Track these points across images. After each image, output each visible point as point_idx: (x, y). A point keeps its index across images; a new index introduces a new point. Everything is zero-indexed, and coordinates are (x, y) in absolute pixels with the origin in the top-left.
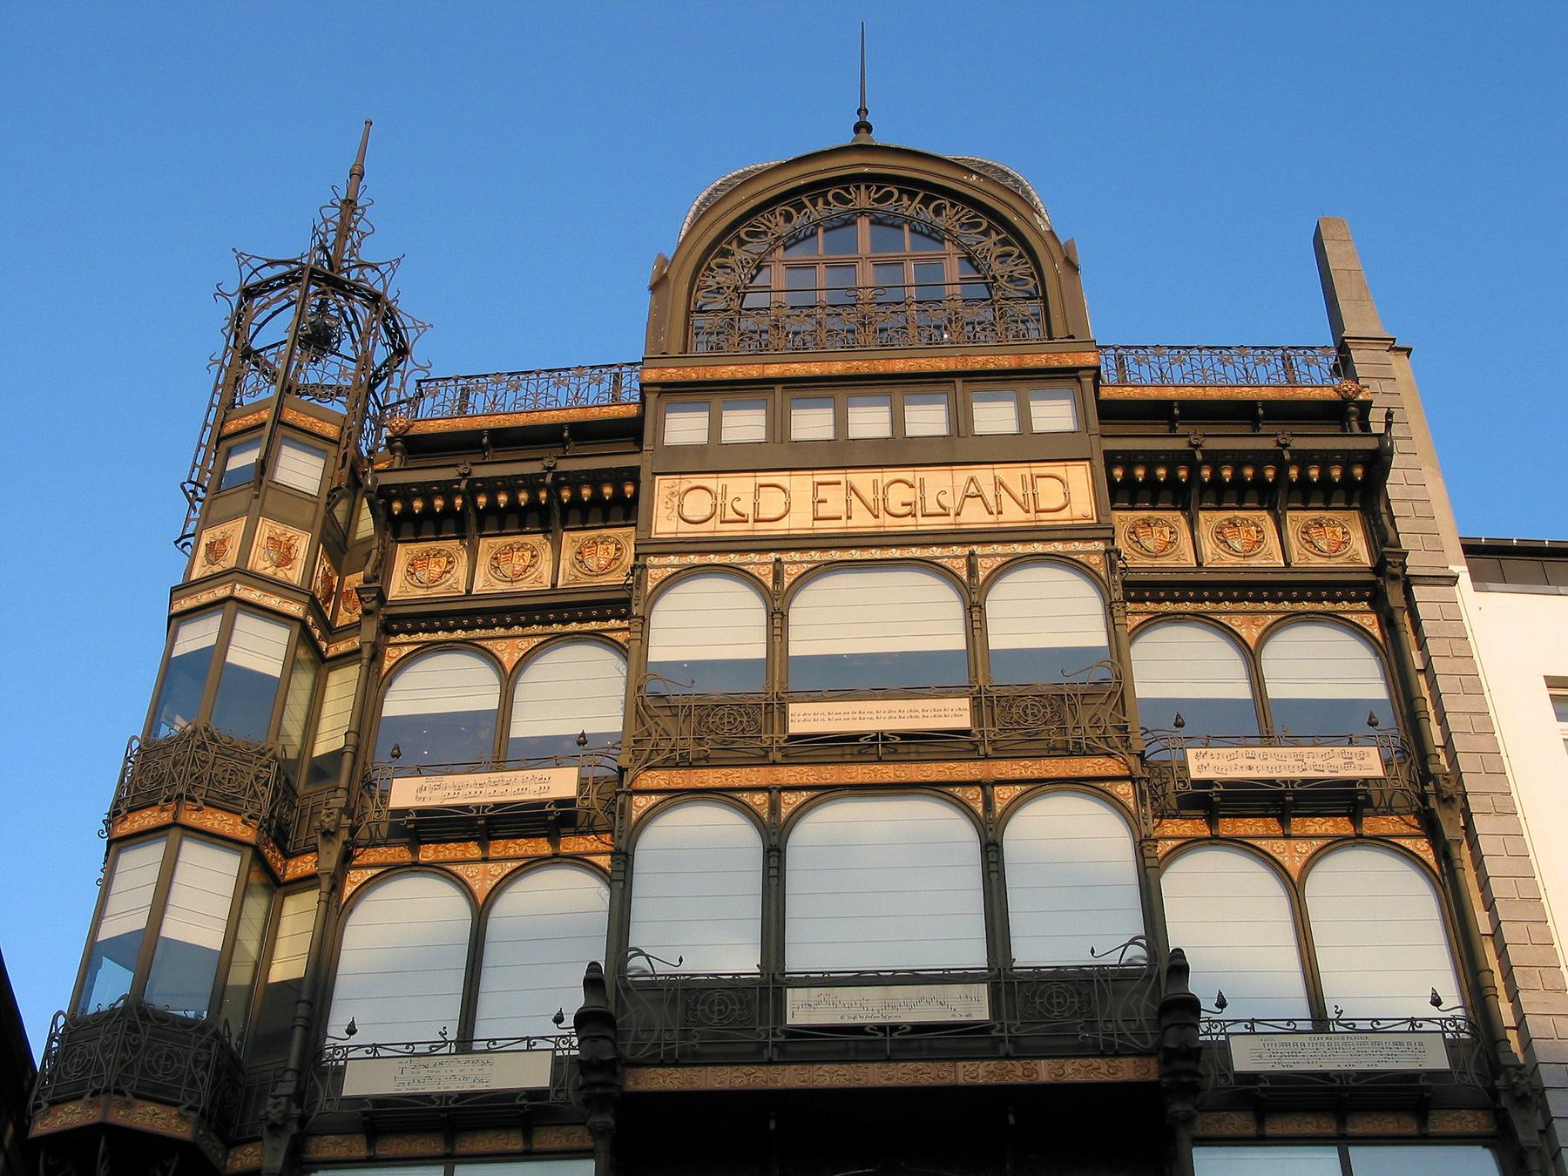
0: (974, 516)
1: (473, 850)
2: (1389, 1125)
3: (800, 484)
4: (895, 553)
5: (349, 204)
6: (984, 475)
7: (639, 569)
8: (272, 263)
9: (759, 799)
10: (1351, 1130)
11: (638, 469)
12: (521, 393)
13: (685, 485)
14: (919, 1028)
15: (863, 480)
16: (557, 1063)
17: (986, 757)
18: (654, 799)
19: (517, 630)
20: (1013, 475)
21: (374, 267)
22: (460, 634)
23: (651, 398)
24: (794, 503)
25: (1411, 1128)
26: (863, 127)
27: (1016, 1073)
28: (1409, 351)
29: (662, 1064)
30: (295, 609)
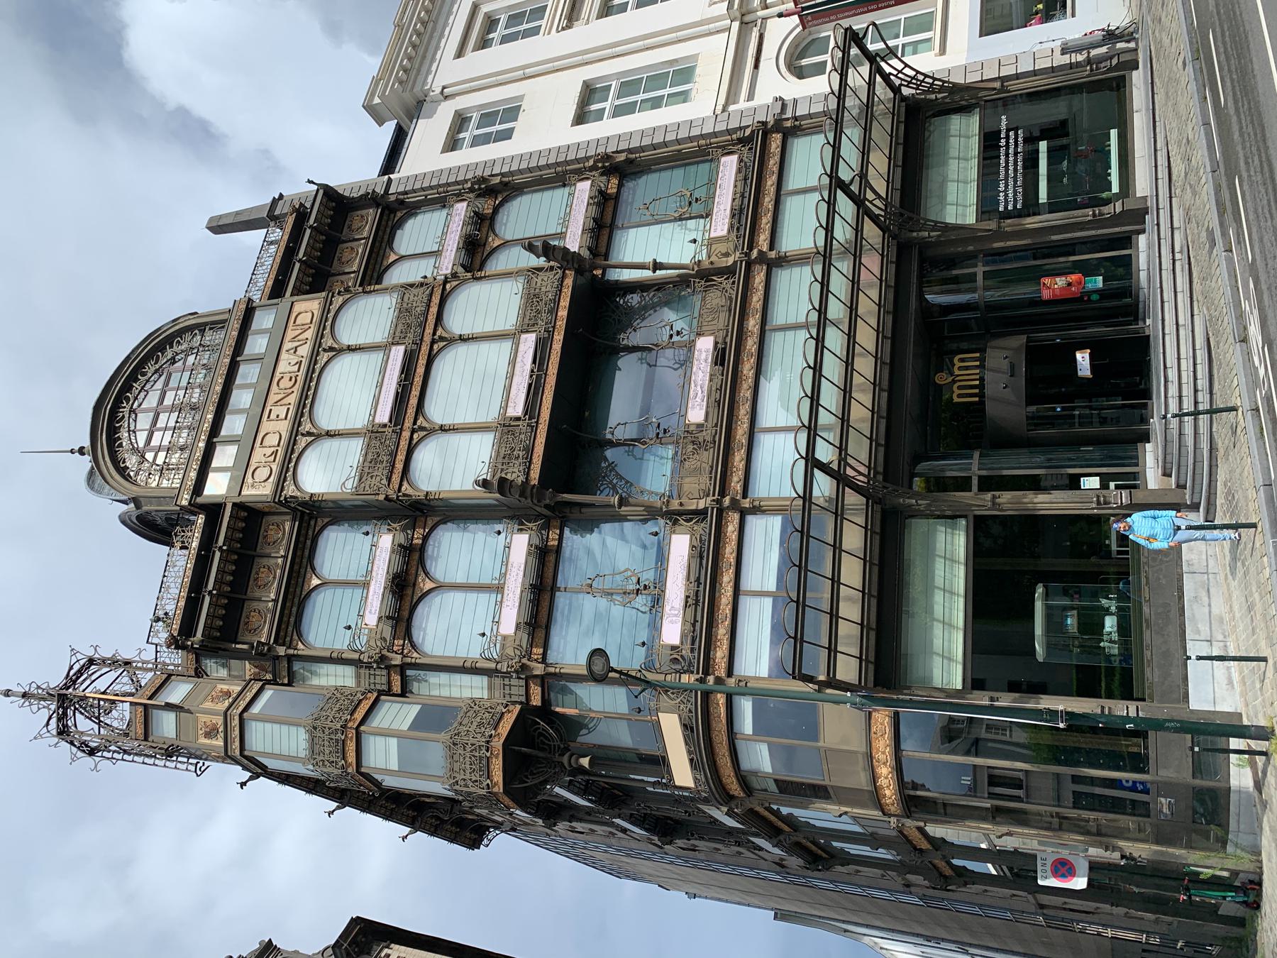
0: (305, 351)
1: (409, 591)
2: (610, 210)
3: (266, 426)
4: (313, 384)
5: (24, 695)
6: (287, 345)
7: (286, 503)
8: (48, 724)
9: (415, 436)
10: (609, 221)
11: (234, 504)
12: (172, 585)
13: (249, 479)
14: (534, 362)
15: (273, 398)
16: (520, 530)
17: (421, 340)
18: (405, 484)
19: (300, 580)
20: (290, 334)
21: (71, 668)
22: (294, 609)
23: (199, 500)
24: (276, 428)
25: (611, 203)
26: (81, 451)
27: (561, 324)
28: (281, 196)
29: (529, 468)
30: (258, 685)
